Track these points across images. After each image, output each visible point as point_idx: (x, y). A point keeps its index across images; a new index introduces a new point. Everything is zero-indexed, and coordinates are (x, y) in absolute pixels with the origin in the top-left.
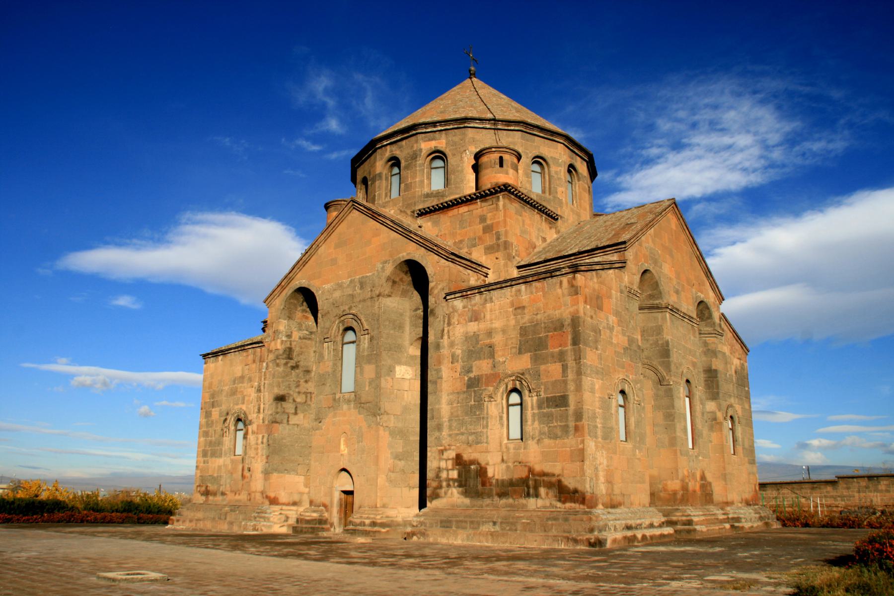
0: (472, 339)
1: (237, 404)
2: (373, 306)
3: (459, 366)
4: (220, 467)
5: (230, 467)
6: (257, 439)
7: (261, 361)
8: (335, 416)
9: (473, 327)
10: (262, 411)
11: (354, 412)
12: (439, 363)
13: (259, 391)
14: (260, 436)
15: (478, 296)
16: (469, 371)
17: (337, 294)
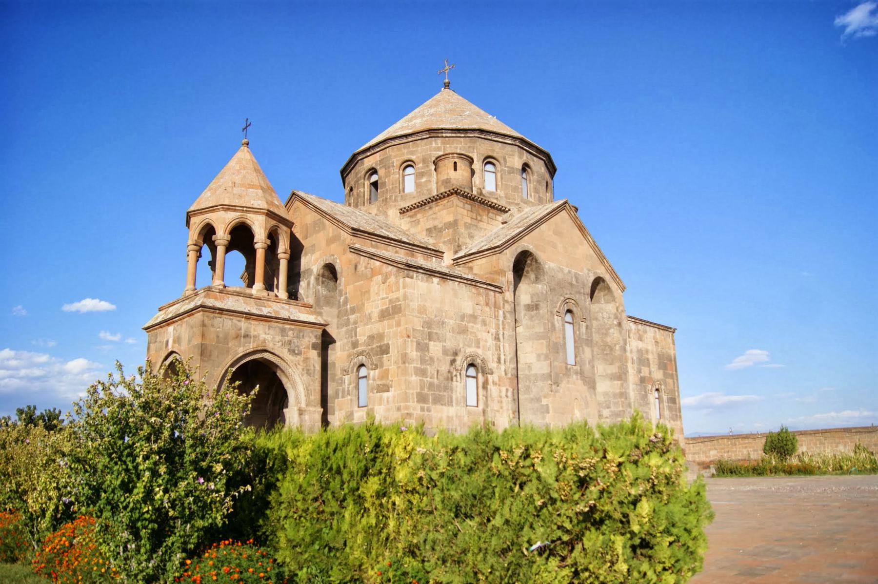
0: (640, 351)
1: (469, 346)
2: (585, 301)
3: (635, 366)
4: (450, 419)
5: (466, 419)
6: (500, 391)
7: (496, 306)
8: (568, 382)
9: (640, 345)
10: (502, 361)
11: (580, 382)
12: (627, 362)
13: (497, 338)
14: (504, 389)
15: (640, 327)
16: (640, 372)
17: (560, 276)
